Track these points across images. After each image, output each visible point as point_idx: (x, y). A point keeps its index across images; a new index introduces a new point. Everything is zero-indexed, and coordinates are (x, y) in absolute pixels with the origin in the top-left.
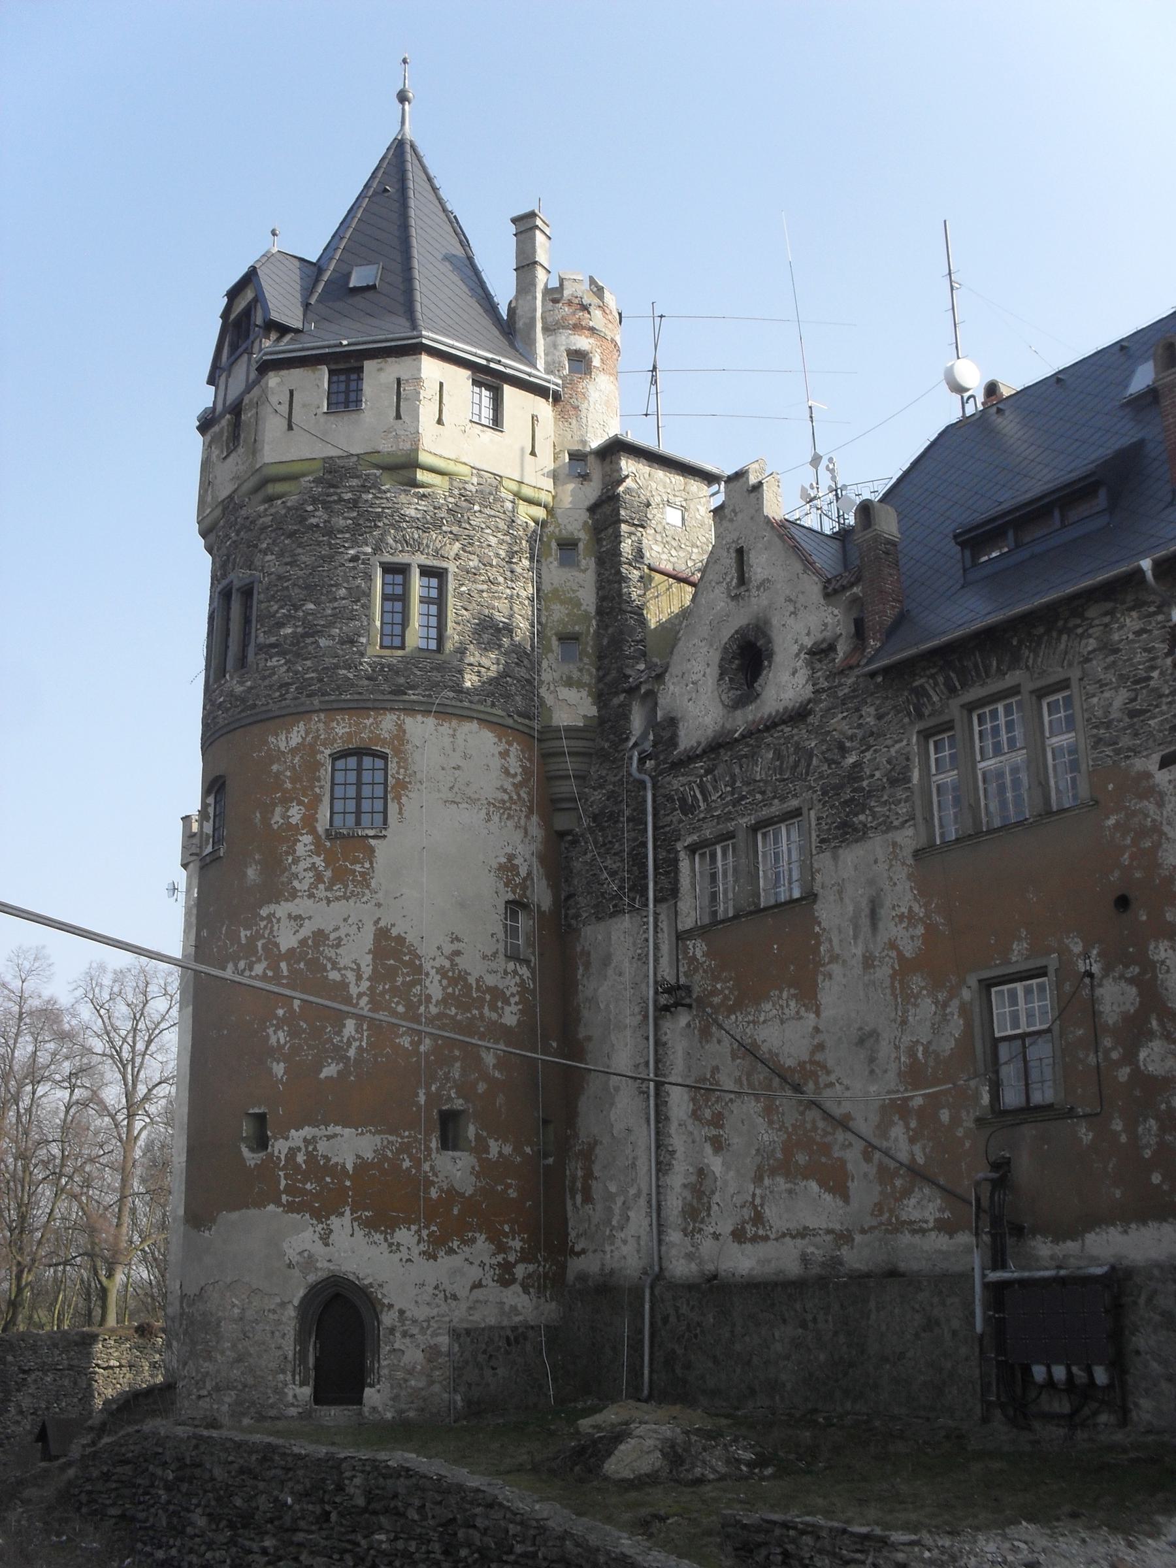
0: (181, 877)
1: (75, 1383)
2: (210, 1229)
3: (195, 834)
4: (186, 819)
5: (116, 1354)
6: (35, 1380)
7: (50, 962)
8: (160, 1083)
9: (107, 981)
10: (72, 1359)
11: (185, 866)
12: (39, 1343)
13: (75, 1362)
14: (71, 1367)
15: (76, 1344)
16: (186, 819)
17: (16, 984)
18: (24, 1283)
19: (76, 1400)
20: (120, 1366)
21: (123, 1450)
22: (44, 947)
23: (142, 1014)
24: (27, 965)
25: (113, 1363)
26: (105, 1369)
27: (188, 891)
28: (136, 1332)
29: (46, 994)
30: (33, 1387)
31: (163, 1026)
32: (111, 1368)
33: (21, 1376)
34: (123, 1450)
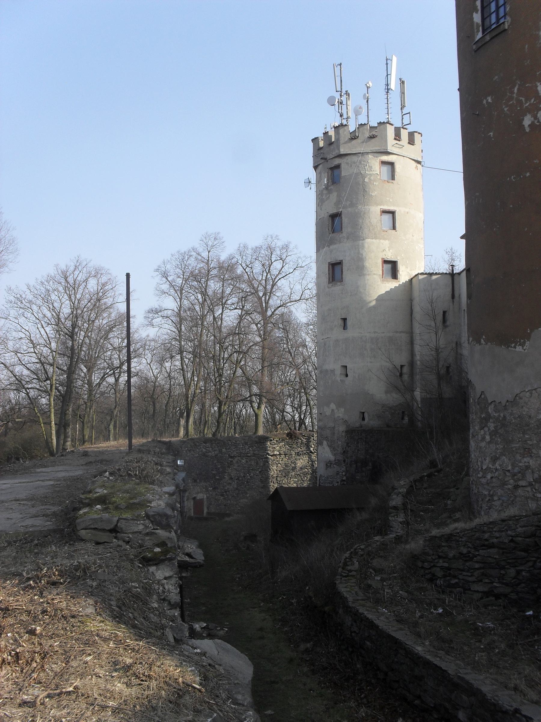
0: (312, 175)
1: (257, 463)
2: (523, 345)
3: (322, 148)
4: (315, 140)
5: (278, 448)
6: (237, 462)
7: (223, 240)
8: (280, 307)
9: (249, 252)
10: (254, 450)
11: (315, 167)
12: (238, 442)
13: (256, 452)
14: (254, 455)
15: (257, 443)
16: (315, 140)
17: (205, 254)
18: (222, 411)
19: (258, 472)
20: (280, 454)
21: (486, 536)
22: (218, 233)
23: (269, 270)
24: (210, 243)
25: (276, 453)
26: (272, 456)
27: (318, 181)
28: (287, 436)
29: (223, 257)
30: (236, 465)
31: (280, 276)
32: (275, 455)
33: (230, 459)
34: (486, 536)
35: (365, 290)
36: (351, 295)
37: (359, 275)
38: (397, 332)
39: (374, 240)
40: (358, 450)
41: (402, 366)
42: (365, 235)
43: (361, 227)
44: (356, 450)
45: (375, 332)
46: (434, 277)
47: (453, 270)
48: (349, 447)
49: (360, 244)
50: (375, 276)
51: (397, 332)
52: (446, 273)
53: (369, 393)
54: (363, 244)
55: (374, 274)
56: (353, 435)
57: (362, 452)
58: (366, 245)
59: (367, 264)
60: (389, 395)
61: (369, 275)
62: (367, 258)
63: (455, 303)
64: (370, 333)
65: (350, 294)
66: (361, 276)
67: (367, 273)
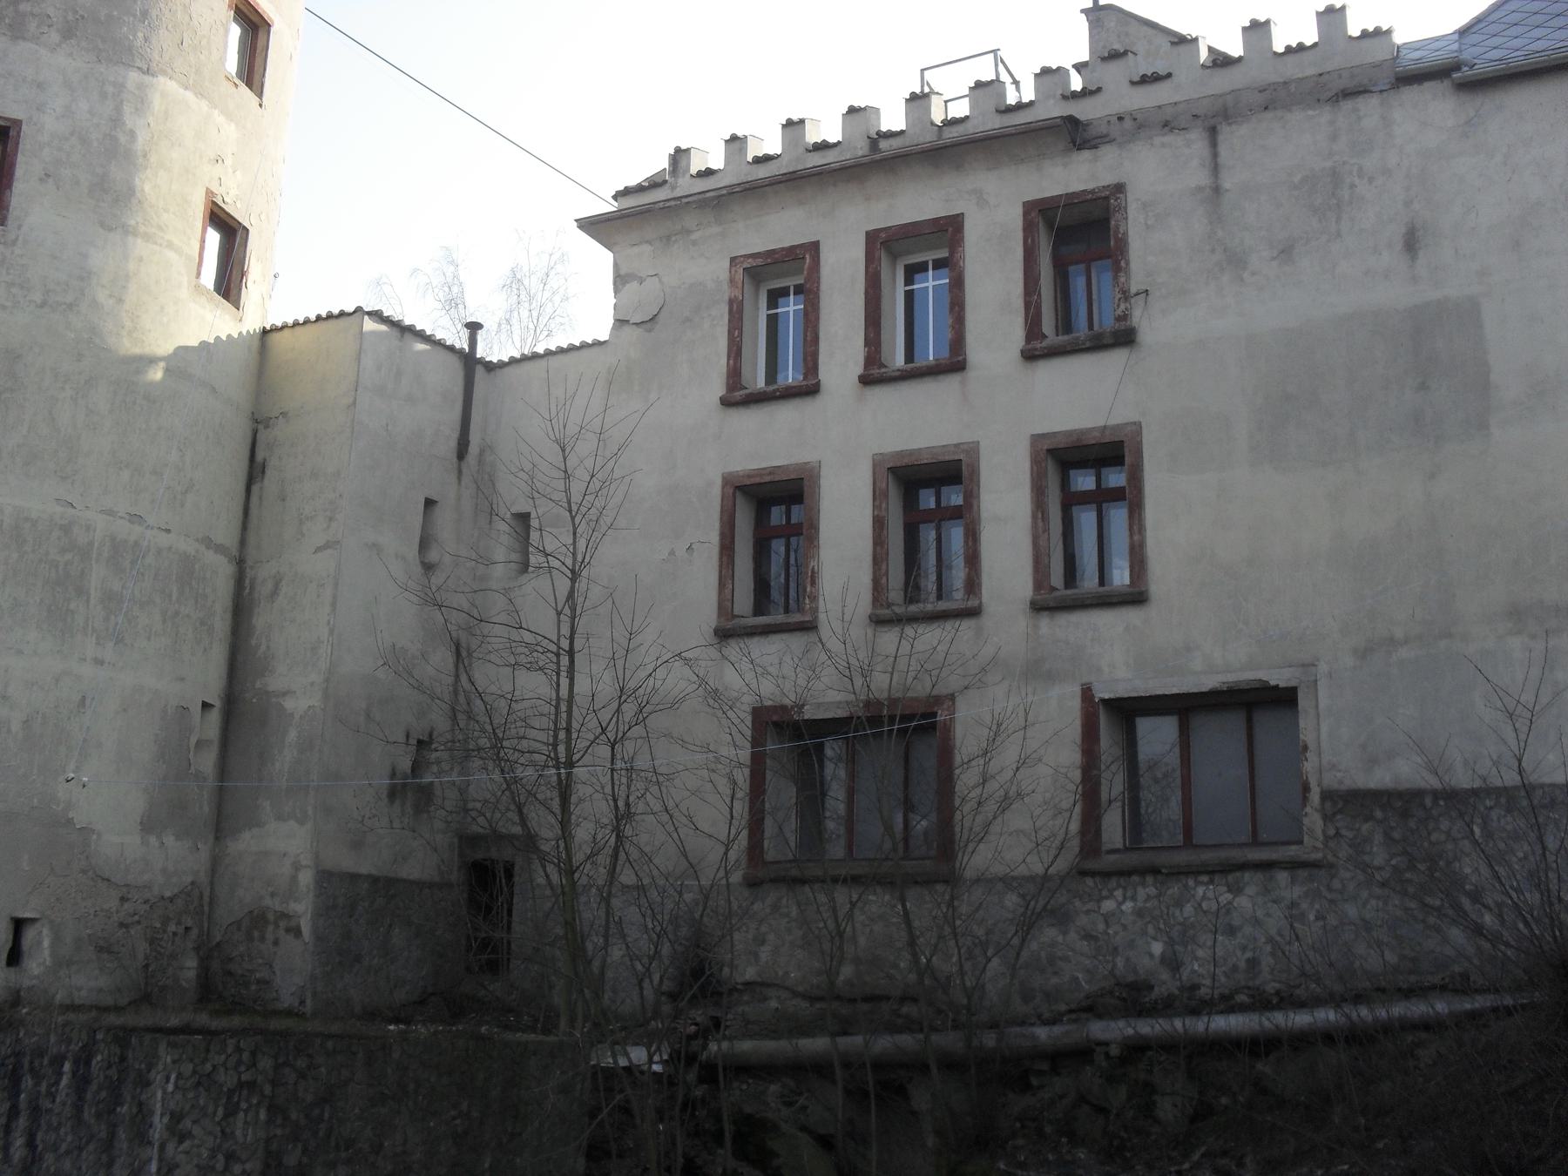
35: (120, 301)
36: (43, 305)
37: (102, 225)
38: (208, 542)
39: (189, 95)
40: (230, 1157)
41: (206, 706)
42: (156, 56)
43: (145, 14)
44: (220, 1157)
45: (135, 518)
46: (421, 346)
47: (473, 342)
48: (182, 1138)
49: (130, 85)
50: (171, 255)
51: (208, 542)
52: (451, 349)
53: (70, 821)
54: (141, 87)
55: (170, 245)
56: (208, 1067)
57: (248, 1166)
58: (157, 103)
59: (147, 188)
60: (153, 840)
61: (147, 237)
62: (153, 159)
63: (463, 483)
64: (110, 513)
65: (37, 297)
66: (110, 229)
67: (142, 229)
